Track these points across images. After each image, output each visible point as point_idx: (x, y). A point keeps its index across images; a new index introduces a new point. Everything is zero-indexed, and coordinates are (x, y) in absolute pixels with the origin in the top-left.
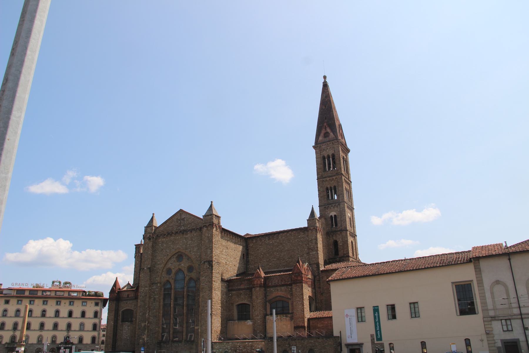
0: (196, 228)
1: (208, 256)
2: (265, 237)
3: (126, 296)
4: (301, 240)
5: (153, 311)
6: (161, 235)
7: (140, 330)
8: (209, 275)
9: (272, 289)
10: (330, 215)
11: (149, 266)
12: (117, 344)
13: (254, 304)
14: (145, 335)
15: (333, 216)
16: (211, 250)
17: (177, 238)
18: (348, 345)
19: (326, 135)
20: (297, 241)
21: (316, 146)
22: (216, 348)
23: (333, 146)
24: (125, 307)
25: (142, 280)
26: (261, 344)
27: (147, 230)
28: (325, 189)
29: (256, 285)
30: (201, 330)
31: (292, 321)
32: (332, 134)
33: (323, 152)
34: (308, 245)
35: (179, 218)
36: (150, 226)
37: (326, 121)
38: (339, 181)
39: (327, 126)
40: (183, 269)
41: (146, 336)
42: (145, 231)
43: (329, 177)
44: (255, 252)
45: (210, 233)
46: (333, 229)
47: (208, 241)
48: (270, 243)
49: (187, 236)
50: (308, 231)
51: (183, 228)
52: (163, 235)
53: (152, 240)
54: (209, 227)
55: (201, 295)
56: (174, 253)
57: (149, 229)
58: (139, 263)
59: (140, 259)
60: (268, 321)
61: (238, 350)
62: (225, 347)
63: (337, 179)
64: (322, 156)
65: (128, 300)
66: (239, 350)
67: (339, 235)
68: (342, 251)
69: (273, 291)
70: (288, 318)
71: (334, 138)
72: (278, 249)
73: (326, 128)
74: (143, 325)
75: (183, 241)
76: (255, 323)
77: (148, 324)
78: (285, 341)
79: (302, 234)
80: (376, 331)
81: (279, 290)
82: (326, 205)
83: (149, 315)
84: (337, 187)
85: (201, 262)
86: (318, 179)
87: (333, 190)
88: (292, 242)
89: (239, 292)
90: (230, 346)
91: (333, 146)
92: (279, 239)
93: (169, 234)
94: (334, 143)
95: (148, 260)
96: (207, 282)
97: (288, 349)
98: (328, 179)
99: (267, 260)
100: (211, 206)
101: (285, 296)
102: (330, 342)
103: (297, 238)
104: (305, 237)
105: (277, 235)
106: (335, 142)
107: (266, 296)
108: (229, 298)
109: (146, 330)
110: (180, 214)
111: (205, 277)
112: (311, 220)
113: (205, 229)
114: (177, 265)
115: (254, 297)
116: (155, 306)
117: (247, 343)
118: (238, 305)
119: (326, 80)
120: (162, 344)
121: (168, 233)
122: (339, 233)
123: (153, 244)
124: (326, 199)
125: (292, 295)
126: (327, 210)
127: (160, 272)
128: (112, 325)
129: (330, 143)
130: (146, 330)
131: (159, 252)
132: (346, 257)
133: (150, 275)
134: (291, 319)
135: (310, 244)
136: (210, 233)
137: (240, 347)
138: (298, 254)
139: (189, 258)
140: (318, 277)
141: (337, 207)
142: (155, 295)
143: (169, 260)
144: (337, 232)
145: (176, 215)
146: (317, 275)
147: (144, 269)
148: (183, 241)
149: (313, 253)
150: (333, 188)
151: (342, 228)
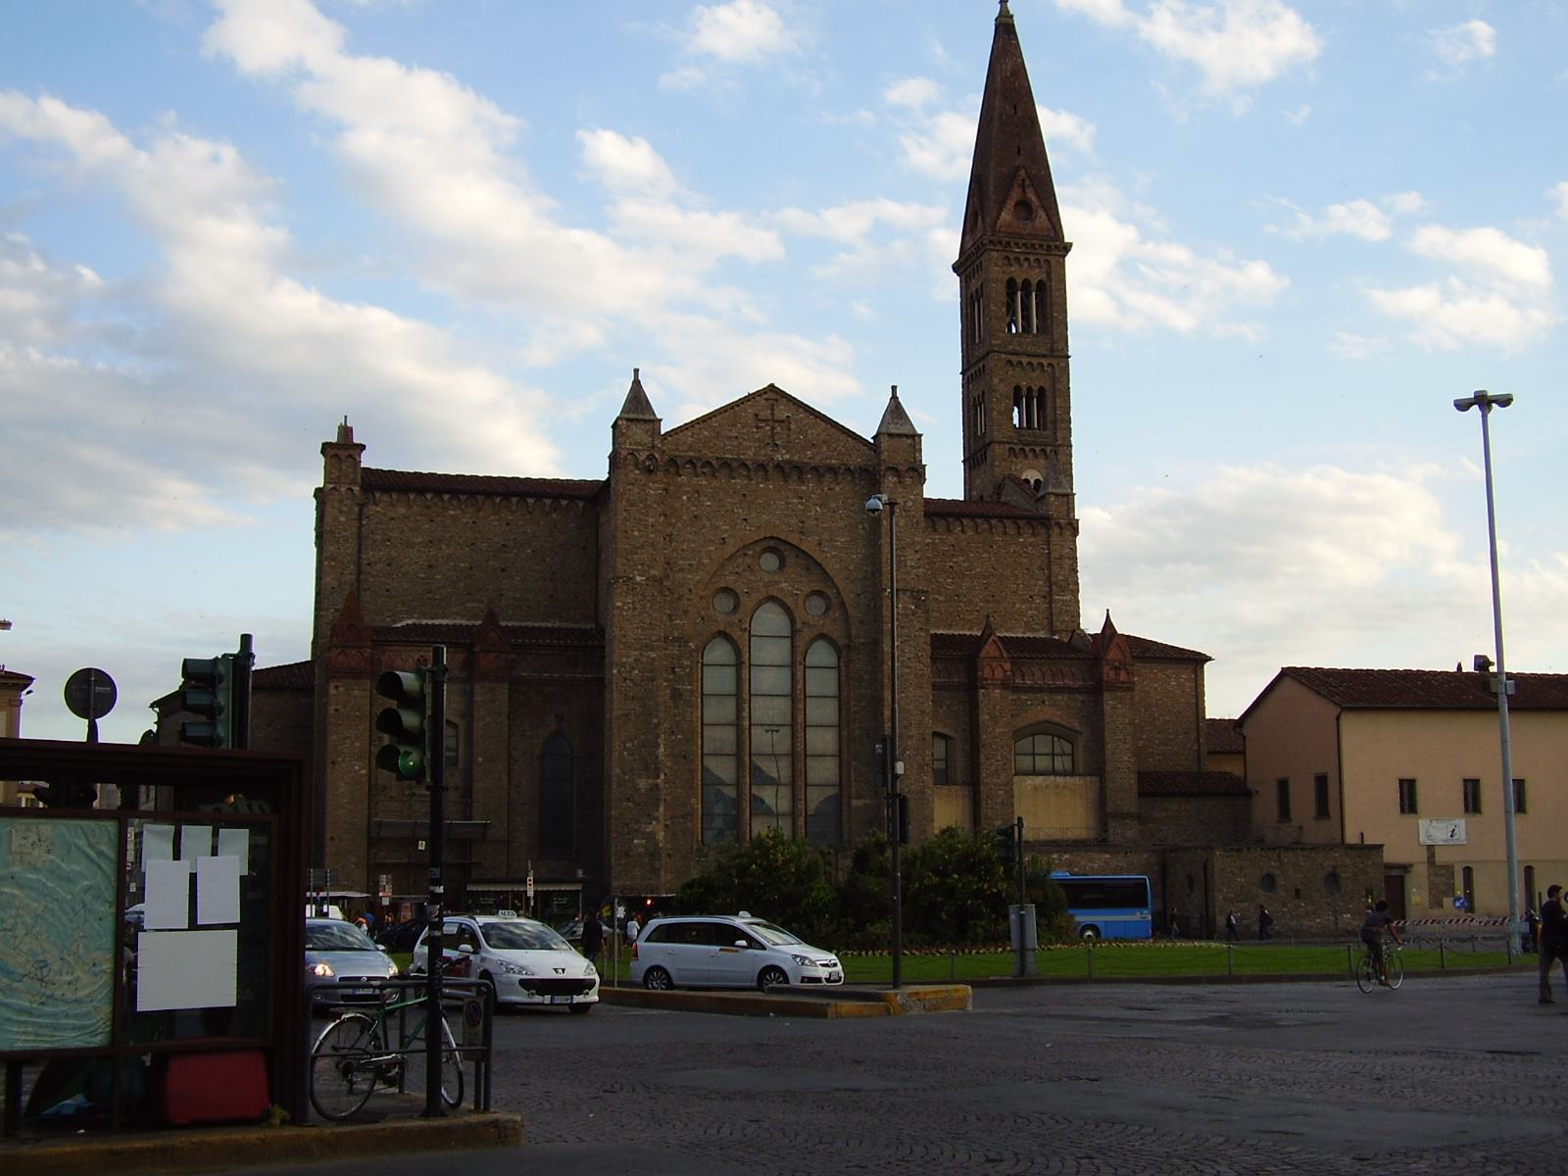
6: (690, 462)
9: (1026, 697)
14: (654, 823)
17: (761, 486)
20: (1015, 552)
26: (1099, 859)
32: (1041, 213)
35: (766, 414)
39: (1027, 182)
41: (661, 826)
45: (912, 497)
50: (1048, 528)
51: (787, 456)
54: (906, 475)
64: (1006, 277)
69: (1029, 702)
71: (1048, 229)
74: (643, 784)
81: (1047, 703)
84: (1048, 394)
96: (909, 659)
98: (1025, 360)
101: (1064, 723)
106: (1057, 247)
110: (766, 399)
116: (677, 718)
126: (1015, 460)
131: (679, 525)
135: (1055, 569)
136: (912, 497)
149: (1065, 598)
150: (1035, 394)
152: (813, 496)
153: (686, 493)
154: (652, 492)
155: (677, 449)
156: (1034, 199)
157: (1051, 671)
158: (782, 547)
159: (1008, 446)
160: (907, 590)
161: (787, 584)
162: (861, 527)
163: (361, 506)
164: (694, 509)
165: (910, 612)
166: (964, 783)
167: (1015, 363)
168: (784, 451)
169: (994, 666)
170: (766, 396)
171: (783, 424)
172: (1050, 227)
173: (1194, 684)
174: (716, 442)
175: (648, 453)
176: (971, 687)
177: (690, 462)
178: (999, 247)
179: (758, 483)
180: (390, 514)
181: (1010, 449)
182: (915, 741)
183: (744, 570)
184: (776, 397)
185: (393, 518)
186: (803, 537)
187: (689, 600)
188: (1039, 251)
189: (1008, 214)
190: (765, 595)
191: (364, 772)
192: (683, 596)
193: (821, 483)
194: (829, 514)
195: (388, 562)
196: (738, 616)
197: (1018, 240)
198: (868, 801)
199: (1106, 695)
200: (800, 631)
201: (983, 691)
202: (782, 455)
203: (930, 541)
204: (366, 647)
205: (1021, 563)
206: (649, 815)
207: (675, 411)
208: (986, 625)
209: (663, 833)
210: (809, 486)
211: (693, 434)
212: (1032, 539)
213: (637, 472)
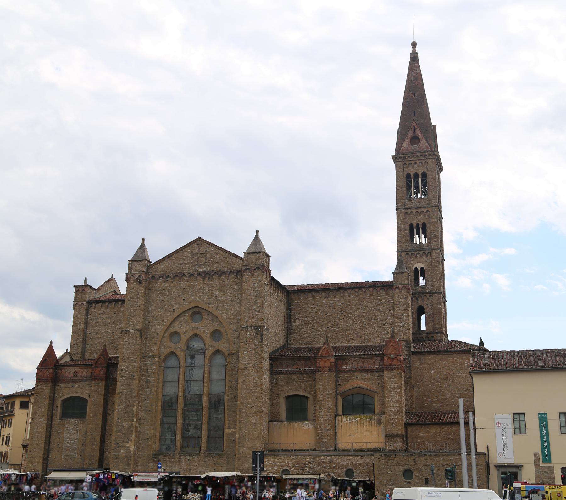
0: (229, 271)
1: (253, 318)
2: (322, 293)
3: (72, 375)
4: (381, 303)
5: (145, 402)
6: (161, 276)
7: (121, 434)
8: (255, 348)
9: (348, 375)
10: (415, 267)
11: (139, 327)
12: (50, 456)
14: (130, 442)
15: (419, 269)
16: (259, 309)
17: (192, 284)
18: (499, 467)
19: (415, 140)
20: (375, 303)
21: (396, 156)
22: (268, 464)
23: (426, 160)
24: (69, 394)
25: (126, 350)
26: (347, 460)
27: (134, 267)
28: (408, 227)
30: (239, 434)
31: (380, 425)
32: (423, 141)
33: (408, 167)
34: (392, 312)
35: (196, 251)
36: (141, 261)
37: (415, 118)
38: (431, 215)
39: (416, 127)
40: (203, 336)
41: (133, 444)
42: (130, 268)
43: (416, 208)
44: (302, 315)
46: (419, 289)
47: (254, 295)
48: (329, 302)
49: (211, 283)
51: (205, 269)
52: (164, 277)
53: (144, 284)
55: (241, 379)
56: (186, 309)
57: (137, 266)
58: (84, 317)
59: (85, 311)
60: (341, 424)
61: (306, 468)
62: (284, 463)
63: (428, 213)
64: (405, 173)
65: (74, 381)
66: (309, 468)
67: (428, 299)
68: (432, 323)
69: (349, 378)
70: (373, 422)
71: (427, 147)
72: (342, 313)
73: (414, 129)
74: (126, 424)
75: (203, 290)
76: (320, 427)
77: (136, 423)
78: (408, 456)
79: (384, 293)
80: (543, 449)
81: (359, 378)
82: (410, 251)
83: (138, 408)
84: (427, 226)
85: (241, 327)
86: (398, 209)
87: (421, 229)
88: (367, 303)
89: (291, 377)
90: (293, 461)
91: (426, 160)
92: (345, 297)
93: (176, 276)
94: (428, 155)
95: (138, 317)
96: (252, 359)
97: (413, 469)
98: (414, 211)
99: (324, 329)
100: (257, 236)
102: (481, 461)
103: (375, 299)
104: (389, 299)
105: (342, 291)
106: (430, 155)
107: (337, 386)
108: (273, 385)
109: (134, 433)
110: (197, 245)
111: (248, 351)
112: (399, 273)
113: (247, 274)
114: (191, 329)
115: (319, 386)
116: (148, 393)
117: (322, 458)
118: (287, 398)
119: (417, 50)
120: (161, 457)
121: (174, 275)
122: (428, 297)
123: (145, 292)
124: (408, 242)
125: (382, 386)
126: (410, 259)
127: (157, 338)
128: (44, 423)
129: (422, 155)
130: (134, 433)
131: (155, 305)
132: (438, 333)
133: (141, 342)
134: (378, 423)
135: (396, 310)
136: (258, 281)
137: (310, 462)
138: (375, 323)
139: (214, 318)
140: (407, 361)
141: (427, 256)
142: (149, 376)
143: (175, 319)
144: (425, 295)
145: (189, 246)
146: (406, 359)
147: (129, 331)
148: (203, 290)
149: (401, 324)
150: (421, 226)
151: (432, 289)
152: (215, 286)
153: (159, 290)
154: (140, 291)
155: (156, 272)
156: (419, 134)
157: (362, 361)
158: (201, 311)
159: (406, 253)
160: (252, 326)
161: (203, 328)
162: (237, 298)
163: (87, 310)
164: (162, 297)
165: (253, 337)
167: (409, 213)
168: (203, 267)
170: (196, 243)
172: (428, 145)
174: (173, 266)
175: (139, 275)
177: (161, 276)
178: (401, 160)
179: (190, 283)
180: (99, 312)
181: (407, 254)
182: (252, 400)
183: (184, 323)
184: (201, 242)
185: (100, 314)
186: (210, 306)
187: (157, 338)
188: (422, 158)
189: (406, 144)
190: (193, 334)
191: (45, 422)
192: (154, 337)
193: (220, 279)
194: (222, 294)
195: (97, 332)
196: (180, 344)
197: (409, 155)
198: (234, 430)
199: (386, 372)
200: (208, 349)
203: (332, 302)
204: (49, 368)
205: (379, 309)
206: (128, 439)
207: (154, 256)
209: (133, 447)
210: (215, 282)
211: (164, 264)
212: (385, 296)
213: (135, 283)
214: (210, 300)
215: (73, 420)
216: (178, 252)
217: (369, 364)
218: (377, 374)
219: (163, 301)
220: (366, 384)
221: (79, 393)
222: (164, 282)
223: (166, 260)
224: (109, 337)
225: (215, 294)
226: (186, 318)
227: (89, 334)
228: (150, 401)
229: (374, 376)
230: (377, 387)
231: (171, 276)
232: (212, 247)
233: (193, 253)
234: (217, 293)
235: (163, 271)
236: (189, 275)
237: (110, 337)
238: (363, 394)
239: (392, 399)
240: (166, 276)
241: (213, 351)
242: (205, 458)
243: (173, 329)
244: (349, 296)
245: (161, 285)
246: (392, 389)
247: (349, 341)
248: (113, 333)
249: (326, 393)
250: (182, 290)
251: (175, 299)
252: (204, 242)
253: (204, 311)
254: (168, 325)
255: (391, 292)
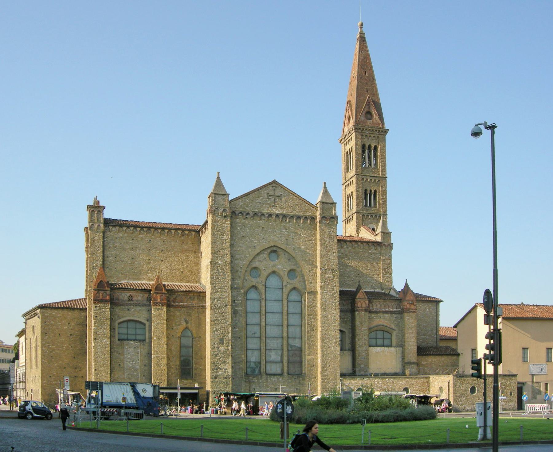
4: (371, 256)
6: (241, 213)
13: (358, 332)
17: (270, 224)
20: (367, 256)
29: (360, 309)
35: (272, 193)
40: (281, 273)
52: (245, 214)
69: (375, 317)
75: (281, 232)
81: (382, 318)
93: (255, 214)
101: (388, 326)
110: (272, 187)
116: (236, 322)
121: (254, 213)
131: (237, 240)
139: (291, 258)
145: (265, 187)
153: (239, 226)
155: (236, 207)
157: (384, 304)
158: (278, 250)
161: (281, 266)
164: (243, 233)
166: (349, 350)
169: (362, 302)
170: (271, 185)
171: (279, 198)
173: (435, 311)
174: (251, 204)
176: (353, 311)
177: (241, 213)
179: (269, 223)
183: (263, 260)
184: (276, 185)
187: (241, 272)
192: (238, 270)
194: (298, 237)
201: (357, 312)
202: (279, 210)
208: (359, 285)
213: (219, 216)
214: (287, 241)
215: (132, 342)
216: (256, 191)
217: (389, 307)
218: (395, 316)
219: (243, 237)
220: (387, 323)
221: (136, 316)
222: (244, 219)
223: (244, 197)
224: (128, 262)
225: (291, 236)
226: (265, 256)
227: (108, 257)
228: (239, 329)
229: (393, 317)
230: (394, 326)
231: (251, 213)
232: (287, 191)
233: (269, 194)
234: (293, 235)
235: (242, 208)
236: (268, 215)
237: (130, 262)
238: (384, 331)
239: (410, 335)
240: (246, 213)
241: (291, 288)
242: (288, 380)
243: (254, 265)
244: (347, 248)
245: (240, 222)
246: (410, 327)
247: (347, 286)
248: (132, 258)
249: (363, 328)
250: (261, 228)
251: (255, 237)
252: (279, 186)
253: (281, 250)
254: (250, 260)
255: (379, 249)
